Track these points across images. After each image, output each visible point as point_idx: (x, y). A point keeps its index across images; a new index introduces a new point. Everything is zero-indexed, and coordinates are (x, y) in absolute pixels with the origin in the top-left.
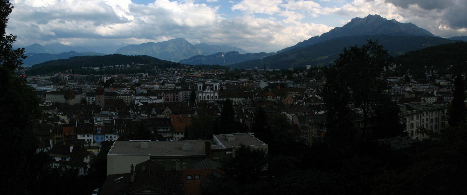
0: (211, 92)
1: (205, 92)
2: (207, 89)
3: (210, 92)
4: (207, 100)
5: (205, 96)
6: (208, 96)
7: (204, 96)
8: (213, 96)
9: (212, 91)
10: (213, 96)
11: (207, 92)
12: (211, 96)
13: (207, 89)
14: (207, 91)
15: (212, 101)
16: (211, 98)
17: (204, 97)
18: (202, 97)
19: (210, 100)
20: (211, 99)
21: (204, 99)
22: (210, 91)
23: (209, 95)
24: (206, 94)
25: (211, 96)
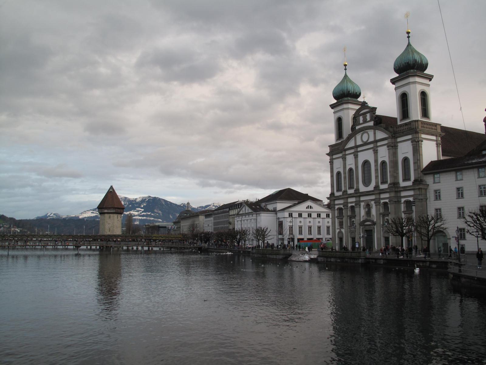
0: (376, 141)
3: (372, 139)
4: (362, 188)
5: (353, 167)
6: (366, 163)
8: (387, 160)
10: (387, 160)
11: (359, 142)
13: (357, 128)
14: (358, 137)
16: (377, 177)
17: (351, 170)
19: (371, 188)
20: (377, 183)
21: (351, 187)
22: (371, 132)
23: (367, 155)
24: (356, 157)
25: (380, 161)
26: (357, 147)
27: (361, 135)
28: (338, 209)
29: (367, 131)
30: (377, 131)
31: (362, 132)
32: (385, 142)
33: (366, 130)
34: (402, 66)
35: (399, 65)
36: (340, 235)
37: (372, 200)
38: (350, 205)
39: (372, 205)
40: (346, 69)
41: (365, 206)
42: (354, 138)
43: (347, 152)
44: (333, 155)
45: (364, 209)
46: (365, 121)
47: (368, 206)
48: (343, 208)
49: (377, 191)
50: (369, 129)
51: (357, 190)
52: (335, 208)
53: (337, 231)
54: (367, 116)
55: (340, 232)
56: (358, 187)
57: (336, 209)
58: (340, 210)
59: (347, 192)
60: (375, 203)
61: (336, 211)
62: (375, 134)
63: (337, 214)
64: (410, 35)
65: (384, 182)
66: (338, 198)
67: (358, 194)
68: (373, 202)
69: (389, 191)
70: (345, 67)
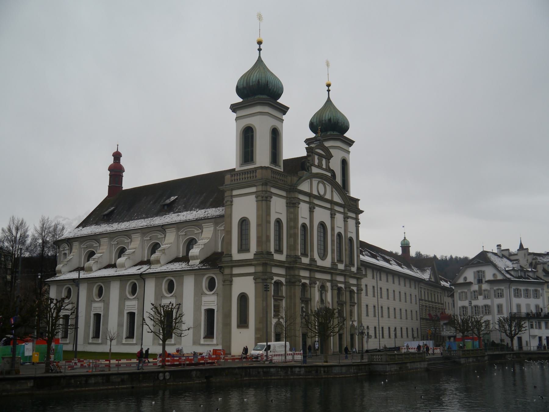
0: (331, 202)
1: (304, 187)
2: (315, 170)
3: (328, 196)
7: (301, 221)
9: (337, 198)
11: (315, 193)
12: (333, 229)
15: (342, 273)
18: (292, 236)
19: (327, 263)
20: (333, 258)
21: (305, 254)
22: (329, 188)
24: (311, 211)
25: (337, 231)
26: (310, 195)
27: (318, 182)
28: (275, 282)
29: (325, 182)
30: (334, 190)
31: (320, 180)
32: (341, 210)
33: (324, 180)
34: (344, 127)
35: (343, 123)
36: (279, 330)
37: (328, 281)
38: (303, 281)
39: (327, 287)
40: (260, 50)
41: (319, 287)
42: (309, 180)
43: (301, 197)
44: (272, 187)
45: (318, 292)
46: (320, 166)
47: (323, 288)
48: (284, 283)
49: (332, 271)
50: (325, 181)
51: (313, 260)
52: (273, 279)
53: (274, 321)
54: (323, 160)
55: (278, 324)
56: (312, 256)
57: (273, 281)
58: (278, 284)
59: (301, 258)
60: (332, 287)
61: (272, 285)
62: (332, 191)
63: (274, 292)
64: (330, 88)
65: (340, 261)
66: (282, 264)
67: (312, 268)
68: (329, 285)
69: (348, 274)
70: (260, 47)
